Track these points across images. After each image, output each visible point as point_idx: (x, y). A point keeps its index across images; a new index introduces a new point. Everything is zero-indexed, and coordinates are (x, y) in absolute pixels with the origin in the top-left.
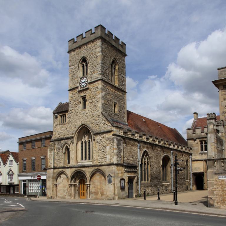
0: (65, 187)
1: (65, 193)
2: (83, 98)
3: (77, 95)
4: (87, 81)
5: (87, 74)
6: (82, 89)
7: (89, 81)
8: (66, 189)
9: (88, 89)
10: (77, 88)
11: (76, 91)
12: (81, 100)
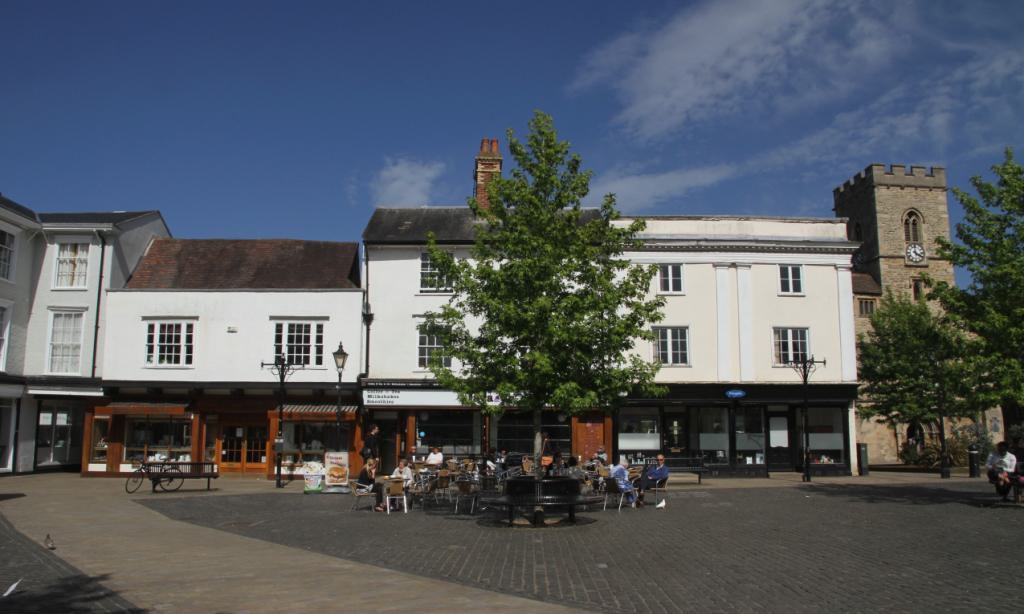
0: (883, 439)
1: (883, 452)
2: (914, 280)
3: (904, 271)
4: (924, 253)
5: (916, 238)
6: (911, 263)
7: (927, 254)
8: (884, 443)
9: (926, 267)
10: (903, 257)
11: (901, 261)
12: (912, 283)
